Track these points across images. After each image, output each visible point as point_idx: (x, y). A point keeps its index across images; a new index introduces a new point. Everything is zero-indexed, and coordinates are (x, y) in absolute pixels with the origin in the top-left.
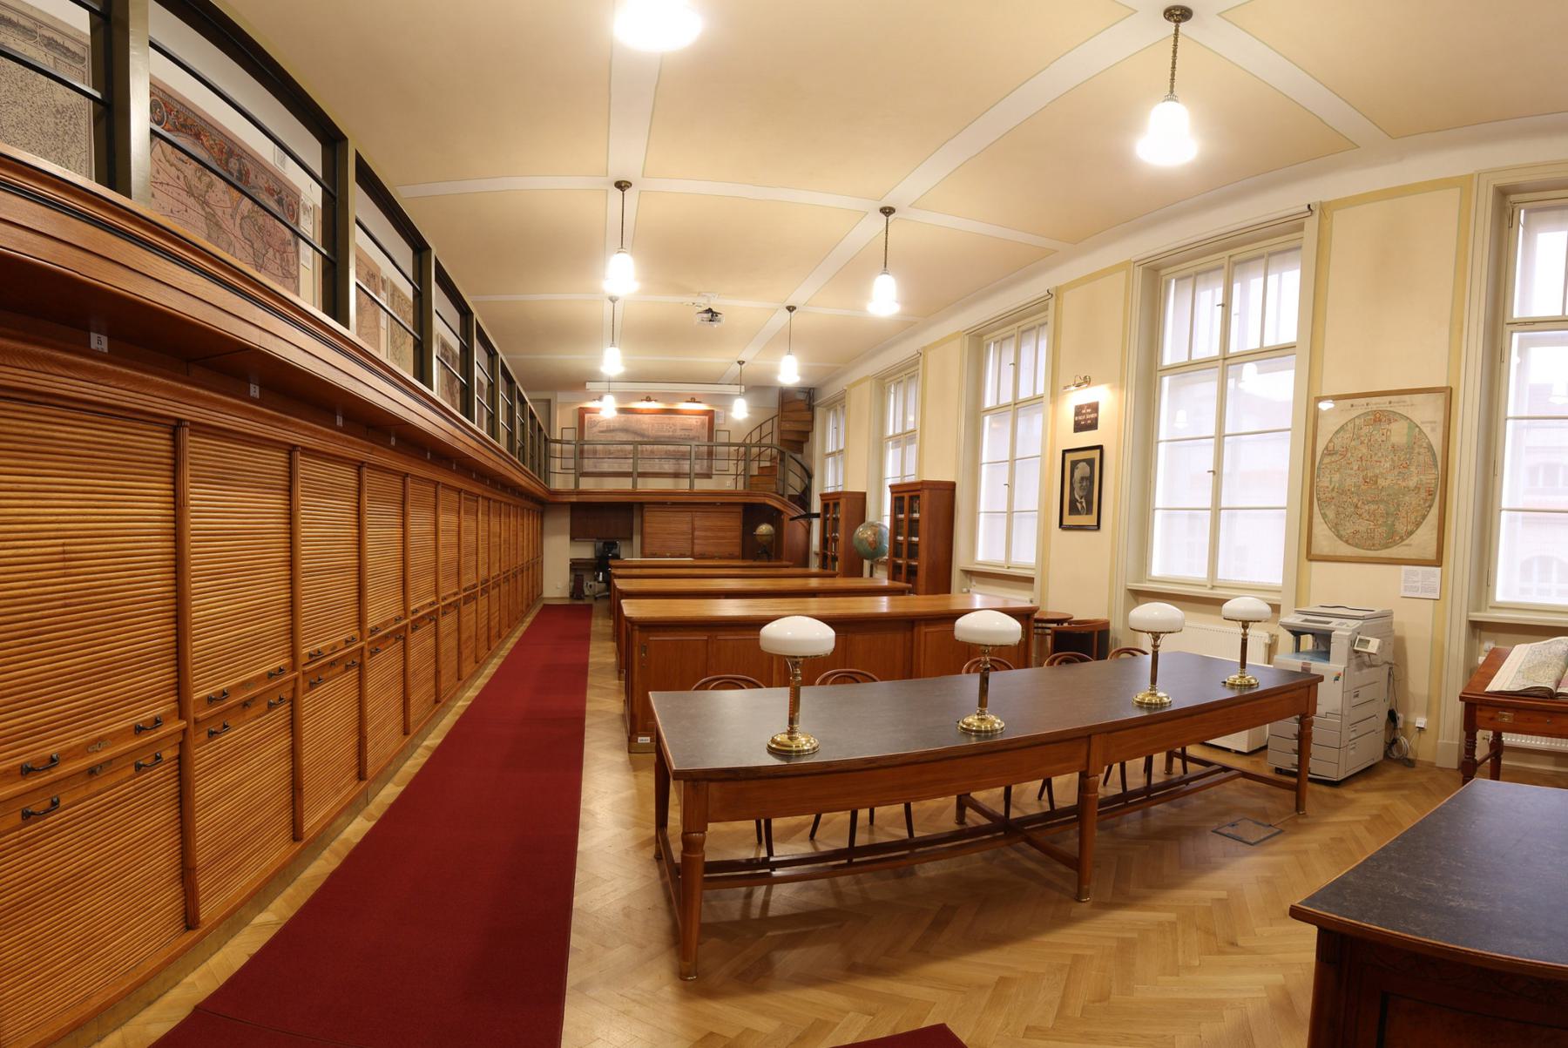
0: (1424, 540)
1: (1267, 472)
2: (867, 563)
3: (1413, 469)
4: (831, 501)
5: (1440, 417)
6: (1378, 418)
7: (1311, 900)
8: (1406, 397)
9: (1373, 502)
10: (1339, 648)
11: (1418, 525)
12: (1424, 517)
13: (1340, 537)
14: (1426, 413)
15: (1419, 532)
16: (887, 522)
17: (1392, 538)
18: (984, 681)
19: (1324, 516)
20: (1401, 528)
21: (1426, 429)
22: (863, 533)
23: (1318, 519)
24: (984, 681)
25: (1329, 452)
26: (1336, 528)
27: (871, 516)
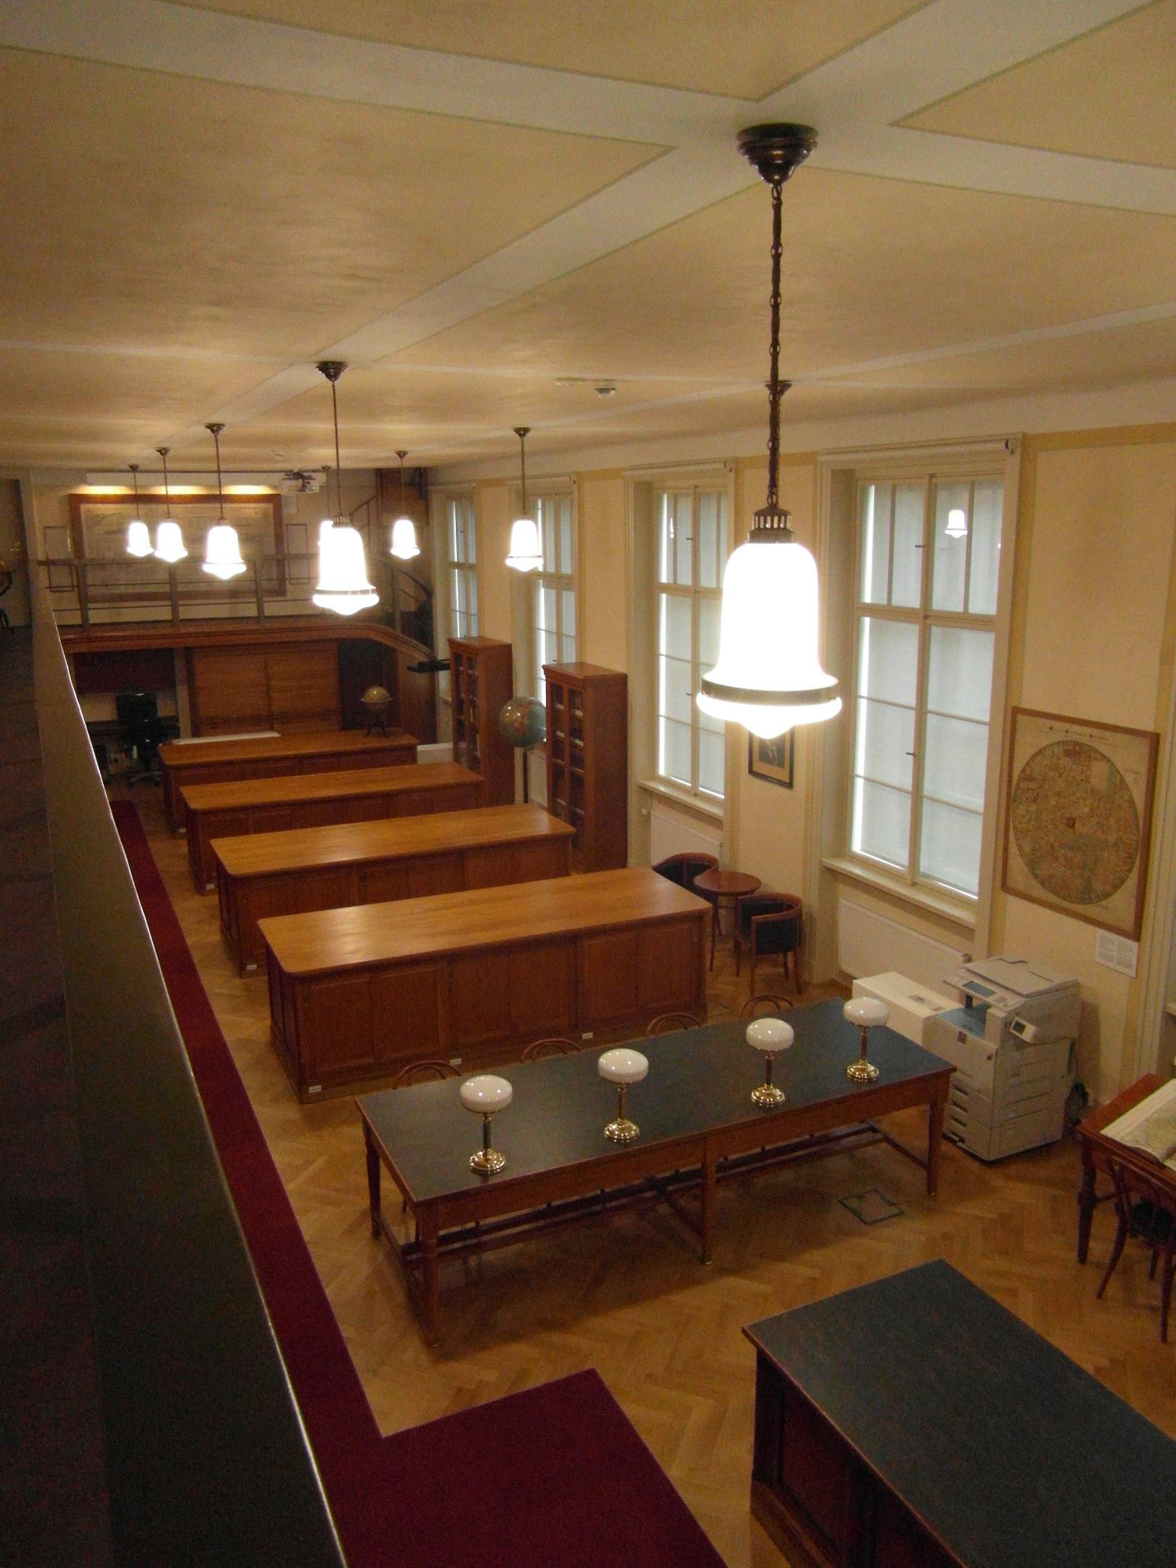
0: (1121, 903)
1: (964, 775)
2: (518, 752)
3: (1112, 821)
4: (463, 654)
5: (1143, 768)
6: (1077, 751)
7: (751, 1327)
8: (1107, 734)
9: (1071, 848)
10: (993, 1028)
11: (1116, 888)
12: (1123, 881)
13: (1036, 876)
14: (1130, 760)
15: (1116, 896)
16: (543, 699)
17: (1088, 895)
18: (984, 723)
19: (1021, 849)
20: (1098, 887)
21: (1129, 778)
22: (511, 714)
23: (1013, 849)
24: (984, 723)
25: (1026, 777)
26: (1032, 865)
27: (520, 690)
